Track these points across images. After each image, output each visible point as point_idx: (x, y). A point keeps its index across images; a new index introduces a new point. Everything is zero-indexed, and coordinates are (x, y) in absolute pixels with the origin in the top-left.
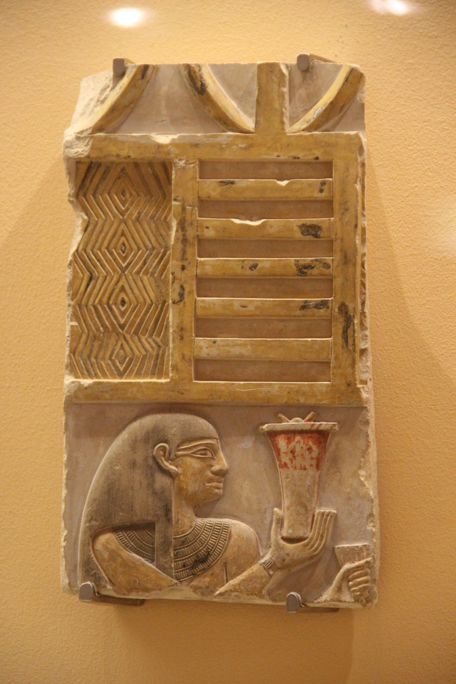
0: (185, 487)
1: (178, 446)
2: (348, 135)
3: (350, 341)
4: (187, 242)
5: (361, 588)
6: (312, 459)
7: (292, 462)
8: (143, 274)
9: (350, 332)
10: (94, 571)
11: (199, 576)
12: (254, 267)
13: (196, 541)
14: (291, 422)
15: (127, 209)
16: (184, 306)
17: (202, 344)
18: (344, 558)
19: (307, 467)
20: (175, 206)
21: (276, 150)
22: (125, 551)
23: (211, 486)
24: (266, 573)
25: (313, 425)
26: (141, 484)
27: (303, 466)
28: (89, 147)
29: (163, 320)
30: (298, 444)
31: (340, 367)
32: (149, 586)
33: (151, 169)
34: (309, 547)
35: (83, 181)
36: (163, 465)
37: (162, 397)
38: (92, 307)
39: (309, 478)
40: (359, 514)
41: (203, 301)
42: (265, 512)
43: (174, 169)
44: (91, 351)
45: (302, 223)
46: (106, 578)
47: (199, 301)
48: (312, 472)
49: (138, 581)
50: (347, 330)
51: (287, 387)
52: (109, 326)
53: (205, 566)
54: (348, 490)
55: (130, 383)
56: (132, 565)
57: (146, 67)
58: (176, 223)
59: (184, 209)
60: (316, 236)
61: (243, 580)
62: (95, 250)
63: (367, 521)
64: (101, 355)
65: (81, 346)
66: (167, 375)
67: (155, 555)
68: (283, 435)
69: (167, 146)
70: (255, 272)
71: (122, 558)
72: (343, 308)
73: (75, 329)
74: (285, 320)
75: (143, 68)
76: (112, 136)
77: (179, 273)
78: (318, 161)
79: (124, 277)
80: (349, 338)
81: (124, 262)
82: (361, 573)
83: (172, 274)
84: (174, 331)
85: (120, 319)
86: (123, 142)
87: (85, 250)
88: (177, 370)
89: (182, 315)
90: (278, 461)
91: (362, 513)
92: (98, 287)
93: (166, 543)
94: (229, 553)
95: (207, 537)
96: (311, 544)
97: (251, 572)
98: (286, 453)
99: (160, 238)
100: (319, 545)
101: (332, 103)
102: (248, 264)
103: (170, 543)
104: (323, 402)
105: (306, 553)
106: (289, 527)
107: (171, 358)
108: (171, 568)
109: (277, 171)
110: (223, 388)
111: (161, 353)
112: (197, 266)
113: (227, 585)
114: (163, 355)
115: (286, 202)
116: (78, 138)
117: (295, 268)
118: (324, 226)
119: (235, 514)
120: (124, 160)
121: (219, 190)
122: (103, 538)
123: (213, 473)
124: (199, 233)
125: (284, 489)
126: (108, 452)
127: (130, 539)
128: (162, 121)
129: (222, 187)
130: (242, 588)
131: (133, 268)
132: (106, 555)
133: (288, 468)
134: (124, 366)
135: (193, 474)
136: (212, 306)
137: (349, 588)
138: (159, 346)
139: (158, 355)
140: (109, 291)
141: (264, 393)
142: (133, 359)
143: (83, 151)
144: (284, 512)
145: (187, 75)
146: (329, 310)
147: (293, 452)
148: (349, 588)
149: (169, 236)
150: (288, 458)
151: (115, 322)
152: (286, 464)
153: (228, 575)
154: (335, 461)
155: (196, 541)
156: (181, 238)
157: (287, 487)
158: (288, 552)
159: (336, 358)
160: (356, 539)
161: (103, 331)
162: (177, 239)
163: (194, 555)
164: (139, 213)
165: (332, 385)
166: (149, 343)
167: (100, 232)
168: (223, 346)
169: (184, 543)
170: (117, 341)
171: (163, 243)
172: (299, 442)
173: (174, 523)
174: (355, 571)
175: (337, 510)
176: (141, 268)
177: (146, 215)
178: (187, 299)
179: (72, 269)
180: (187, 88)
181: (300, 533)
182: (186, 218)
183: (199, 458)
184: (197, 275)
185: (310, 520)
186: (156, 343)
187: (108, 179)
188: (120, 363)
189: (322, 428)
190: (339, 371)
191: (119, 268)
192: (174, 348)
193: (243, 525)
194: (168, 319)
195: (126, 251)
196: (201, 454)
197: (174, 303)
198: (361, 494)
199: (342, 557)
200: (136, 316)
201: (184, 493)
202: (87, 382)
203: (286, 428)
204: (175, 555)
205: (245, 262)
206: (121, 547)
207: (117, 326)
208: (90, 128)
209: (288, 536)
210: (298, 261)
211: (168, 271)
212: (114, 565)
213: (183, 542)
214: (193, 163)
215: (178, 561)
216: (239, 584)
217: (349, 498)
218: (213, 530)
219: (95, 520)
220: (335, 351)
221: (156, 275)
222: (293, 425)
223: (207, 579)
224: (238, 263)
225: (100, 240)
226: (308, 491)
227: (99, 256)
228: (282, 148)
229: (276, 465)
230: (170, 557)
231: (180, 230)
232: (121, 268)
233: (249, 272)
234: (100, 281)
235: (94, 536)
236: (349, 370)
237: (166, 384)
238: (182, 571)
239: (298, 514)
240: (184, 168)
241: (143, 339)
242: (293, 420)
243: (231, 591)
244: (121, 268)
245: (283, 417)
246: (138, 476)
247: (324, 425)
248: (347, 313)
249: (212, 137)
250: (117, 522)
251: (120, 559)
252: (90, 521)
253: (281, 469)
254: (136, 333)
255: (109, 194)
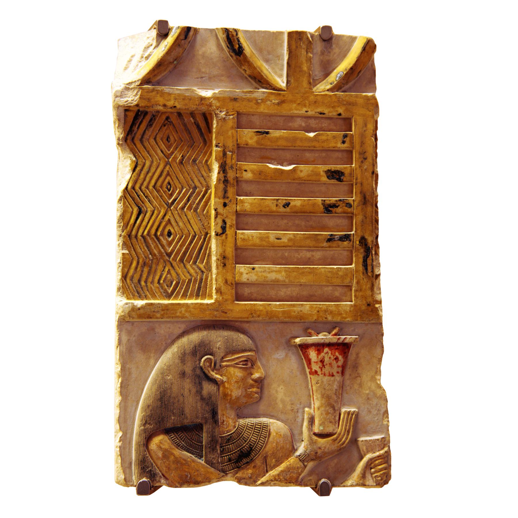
0: (229, 393)
1: (223, 358)
2: (366, 96)
3: (369, 268)
4: (228, 183)
5: (381, 474)
6: (338, 367)
7: (322, 370)
8: (187, 209)
9: (369, 261)
10: (150, 469)
11: (243, 469)
12: (287, 205)
13: (240, 439)
14: (321, 336)
15: (172, 153)
16: (226, 238)
17: (242, 270)
18: (367, 449)
19: (335, 374)
20: (216, 151)
21: (305, 106)
22: (177, 450)
23: (251, 392)
24: (302, 464)
25: (339, 339)
26: (190, 391)
27: (331, 374)
28: (138, 97)
29: (206, 249)
30: (326, 355)
31: (361, 290)
32: (199, 479)
33: (193, 119)
34: (338, 440)
35: (131, 127)
36: (209, 375)
37: (207, 316)
38: (140, 237)
39: (336, 383)
40: (376, 411)
41: (242, 234)
42: (298, 412)
43: (215, 119)
44: (141, 275)
45: (327, 169)
46: (161, 474)
47: (239, 233)
48: (338, 378)
49: (189, 476)
50: (366, 259)
51: (316, 307)
52: (157, 254)
53: (248, 460)
54: (367, 392)
55: (179, 304)
56: (184, 462)
57: (189, 29)
58: (218, 166)
59: (225, 154)
60: (340, 180)
61: (282, 471)
62: (143, 188)
63: (383, 417)
64: (150, 279)
65: (132, 271)
66: (211, 297)
67: (204, 452)
68: (313, 347)
69: (209, 98)
70: (288, 209)
71: (174, 456)
72: (363, 241)
73: (127, 256)
74: (312, 251)
75: (186, 29)
76: (159, 88)
77: (221, 210)
78: (340, 117)
79: (170, 212)
80: (368, 266)
81: (170, 199)
82: (381, 462)
83: (215, 210)
84: (218, 259)
85: (167, 248)
86: (169, 94)
87: (133, 188)
88: (221, 293)
89: (225, 246)
90: (308, 368)
91: (379, 410)
92: (146, 220)
93: (213, 442)
94: (269, 448)
95: (257, 440)
96: (339, 438)
97: (288, 463)
98: (317, 362)
99: (202, 179)
100: (347, 439)
101: (351, 68)
102: (282, 203)
103: (217, 441)
104: (347, 319)
105: (334, 447)
106: (320, 425)
107: (214, 282)
108: (218, 463)
109: (303, 124)
110: (261, 308)
111: (204, 278)
112: (237, 204)
113: (267, 475)
114: (206, 279)
115: (312, 150)
116: (127, 89)
117: (322, 206)
118: (347, 172)
119: (272, 414)
120: (170, 110)
121: (255, 138)
122: (156, 440)
123: (253, 380)
124: (238, 175)
125: (314, 392)
126: (158, 363)
127: (181, 439)
128: (202, 78)
129: (258, 136)
130: (281, 477)
131: (178, 204)
132: (160, 454)
133: (318, 375)
134: (171, 288)
135: (236, 382)
136: (251, 238)
137: (372, 474)
138: (202, 272)
139: (201, 279)
140: (157, 224)
141: (296, 312)
142: (179, 283)
143: (132, 100)
144: (314, 411)
145: (225, 39)
146: (351, 242)
147: (322, 361)
148: (372, 474)
149: (210, 177)
150: (318, 367)
151: (162, 250)
152: (316, 372)
153: (268, 467)
154: (355, 367)
155: (240, 439)
156: (223, 179)
157: (317, 390)
158: (319, 446)
159: (358, 283)
160: (375, 433)
161: (151, 258)
162: (219, 180)
163: (238, 451)
164: (182, 156)
165: (355, 305)
166: (194, 269)
167: (148, 173)
168: (261, 272)
169: (229, 439)
170: (164, 267)
171: (204, 183)
172: (327, 353)
173: (220, 424)
174: (377, 460)
175: (359, 408)
176: (185, 204)
177: (189, 158)
178: (229, 231)
179: (122, 204)
180: (223, 50)
181: (330, 429)
182: (227, 162)
183: (241, 368)
184: (236, 211)
185: (337, 418)
186: (200, 269)
187: (154, 126)
188: (167, 286)
189: (347, 341)
190: (361, 294)
191: (166, 204)
192: (218, 274)
193: (279, 423)
194: (210, 248)
195: (172, 189)
196: (243, 365)
197: (217, 234)
198: (378, 395)
199: (364, 448)
200: (182, 246)
201: (229, 398)
202: (140, 303)
203: (316, 341)
204: (222, 452)
205: (279, 201)
206: (173, 447)
207: (165, 254)
208: (138, 81)
209: (320, 432)
210: (324, 201)
211: (210, 207)
212: (167, 462)
213: (229, 440)
214: (232, 115)
215: (224, 456)
216: (279, 475)
217: (368, 399)
218: (255, 429)
219: (149, 424)
220: (356, 277)
221: (198, 210)
222: (322, 339)
223: (250, 471)
224: (273, 202)
225: (148, 179)
226: (336, 394)
227: (147, 193)
228: (310, 105)
229: (305, 371)
230: (217, 453)
231: (221, 172)
232: (167, 204)
233: (282, 209)
234: (148, 215)
235: (147, 438)
236: (369, 293)
237: (211, 304)
238: (227, 465)
239: (327, 413)
240: (224, 118)
241: (188, 266)
242: (321, 334)
243: (272, 480)
244: (167, 204)
245: (313, 332)
246: (188, 385)
247: (349, 338)
248: (366, 245)
249: (249, 93)
250: (169, 425)
251: (173, 457)
252: (144, 425)
253: (311, 376)
254: (182, 260)
255: (155, 139)
